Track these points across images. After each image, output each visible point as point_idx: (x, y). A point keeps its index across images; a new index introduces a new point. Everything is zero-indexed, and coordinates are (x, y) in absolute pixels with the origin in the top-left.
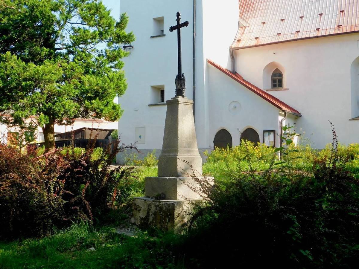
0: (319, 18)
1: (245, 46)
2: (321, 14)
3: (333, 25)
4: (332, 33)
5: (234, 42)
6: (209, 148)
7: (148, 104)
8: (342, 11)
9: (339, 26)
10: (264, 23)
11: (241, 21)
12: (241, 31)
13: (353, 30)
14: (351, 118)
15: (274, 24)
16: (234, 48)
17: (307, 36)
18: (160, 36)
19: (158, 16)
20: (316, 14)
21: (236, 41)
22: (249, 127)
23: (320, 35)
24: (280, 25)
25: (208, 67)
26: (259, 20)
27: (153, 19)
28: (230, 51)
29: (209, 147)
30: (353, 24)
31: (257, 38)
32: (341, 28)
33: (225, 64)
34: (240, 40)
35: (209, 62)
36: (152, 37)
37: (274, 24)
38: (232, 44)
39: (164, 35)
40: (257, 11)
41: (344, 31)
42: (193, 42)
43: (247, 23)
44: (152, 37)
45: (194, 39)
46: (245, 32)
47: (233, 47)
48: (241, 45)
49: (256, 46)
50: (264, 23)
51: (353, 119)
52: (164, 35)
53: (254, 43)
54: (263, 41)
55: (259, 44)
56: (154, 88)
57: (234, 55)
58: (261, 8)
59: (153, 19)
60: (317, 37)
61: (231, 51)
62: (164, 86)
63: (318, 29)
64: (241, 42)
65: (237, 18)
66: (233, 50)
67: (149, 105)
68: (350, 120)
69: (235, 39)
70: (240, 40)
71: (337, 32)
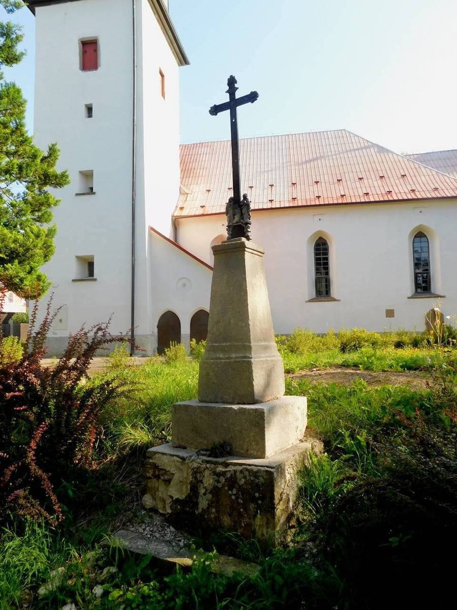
0: (270, 189)
1: (190, 214)
2: (272, 186)
3: (286, 197)
4: (287, 205)
5: (176, 210)
6: (152, 335)
7: (72, 279)
8: (294, 184)
9: (294, 199)
10: (209, 191)
11: (182, 186)
12: (183, 198)
13: (309, 204)
14: (307, 300)
15: (220, 193)
16: (177, 216)
17: (261, 207)
18: (88, 194)
19: (85, 168)
20: (266, 185)
21: (178, 208)
22: (202, 309)
23: (274, 207)
24: (228, 194)
25: (150, 236)
26: (203, 187)
27: (80, 172)
28: (172, 218)
29: (151, 333)
30: (308, 197)
31: (202, 207)
32: (296, 201)
33: (168, 232)
34: (183, 208)
35: (152, 229)
36: (77, 195)
37: (220, 193)
38: (174, 212)
39: (94, 193)
40: (200, 178)
41: (300, 204)
42: (133, 203)
43: (189, 189)
44: (77, 195)
45: (133, 200)
46: (188, 199)
47: (175, 215)
48: (184, 213)
49: (203, 215)
50: (209, 191)
51: (310, 301)
52: (94, 193)
53: (201, 211)
54: (209, 210)
55: (206, 213)
56: (80, 259)
57: (176, 223)
58: (204, 175)
59: (80, 172)
60: (272, 209)
61: (174, 219)
62: (93, 257)
63: (271, 201)
64: (184, 210)
65: (179, 184)
66: (176, 219)
67: (73, 281)
68: (306, 302)
69: (177, 207)
70: (183, 208)
71: (292, 205)
